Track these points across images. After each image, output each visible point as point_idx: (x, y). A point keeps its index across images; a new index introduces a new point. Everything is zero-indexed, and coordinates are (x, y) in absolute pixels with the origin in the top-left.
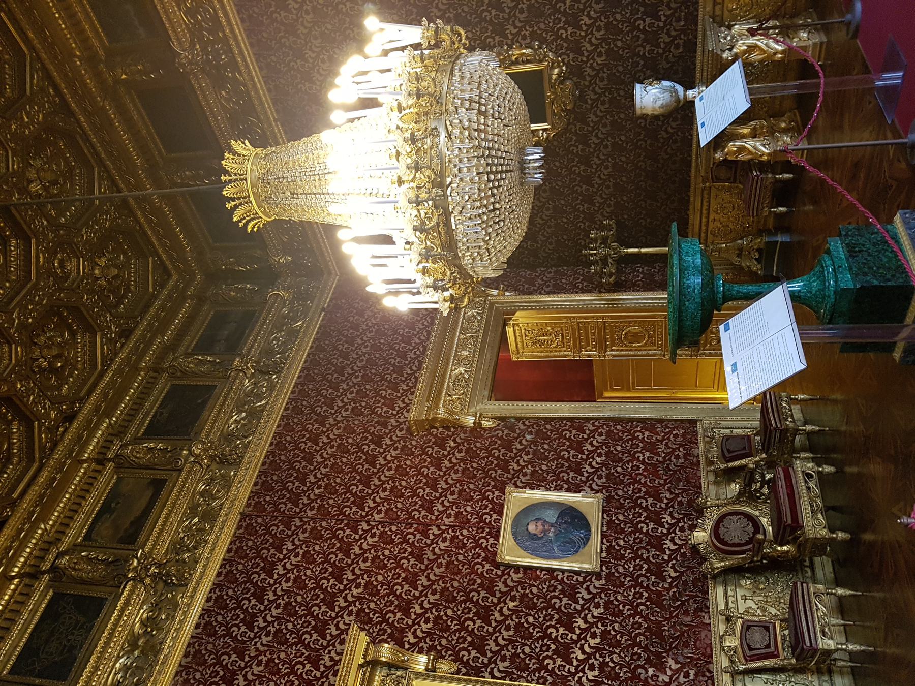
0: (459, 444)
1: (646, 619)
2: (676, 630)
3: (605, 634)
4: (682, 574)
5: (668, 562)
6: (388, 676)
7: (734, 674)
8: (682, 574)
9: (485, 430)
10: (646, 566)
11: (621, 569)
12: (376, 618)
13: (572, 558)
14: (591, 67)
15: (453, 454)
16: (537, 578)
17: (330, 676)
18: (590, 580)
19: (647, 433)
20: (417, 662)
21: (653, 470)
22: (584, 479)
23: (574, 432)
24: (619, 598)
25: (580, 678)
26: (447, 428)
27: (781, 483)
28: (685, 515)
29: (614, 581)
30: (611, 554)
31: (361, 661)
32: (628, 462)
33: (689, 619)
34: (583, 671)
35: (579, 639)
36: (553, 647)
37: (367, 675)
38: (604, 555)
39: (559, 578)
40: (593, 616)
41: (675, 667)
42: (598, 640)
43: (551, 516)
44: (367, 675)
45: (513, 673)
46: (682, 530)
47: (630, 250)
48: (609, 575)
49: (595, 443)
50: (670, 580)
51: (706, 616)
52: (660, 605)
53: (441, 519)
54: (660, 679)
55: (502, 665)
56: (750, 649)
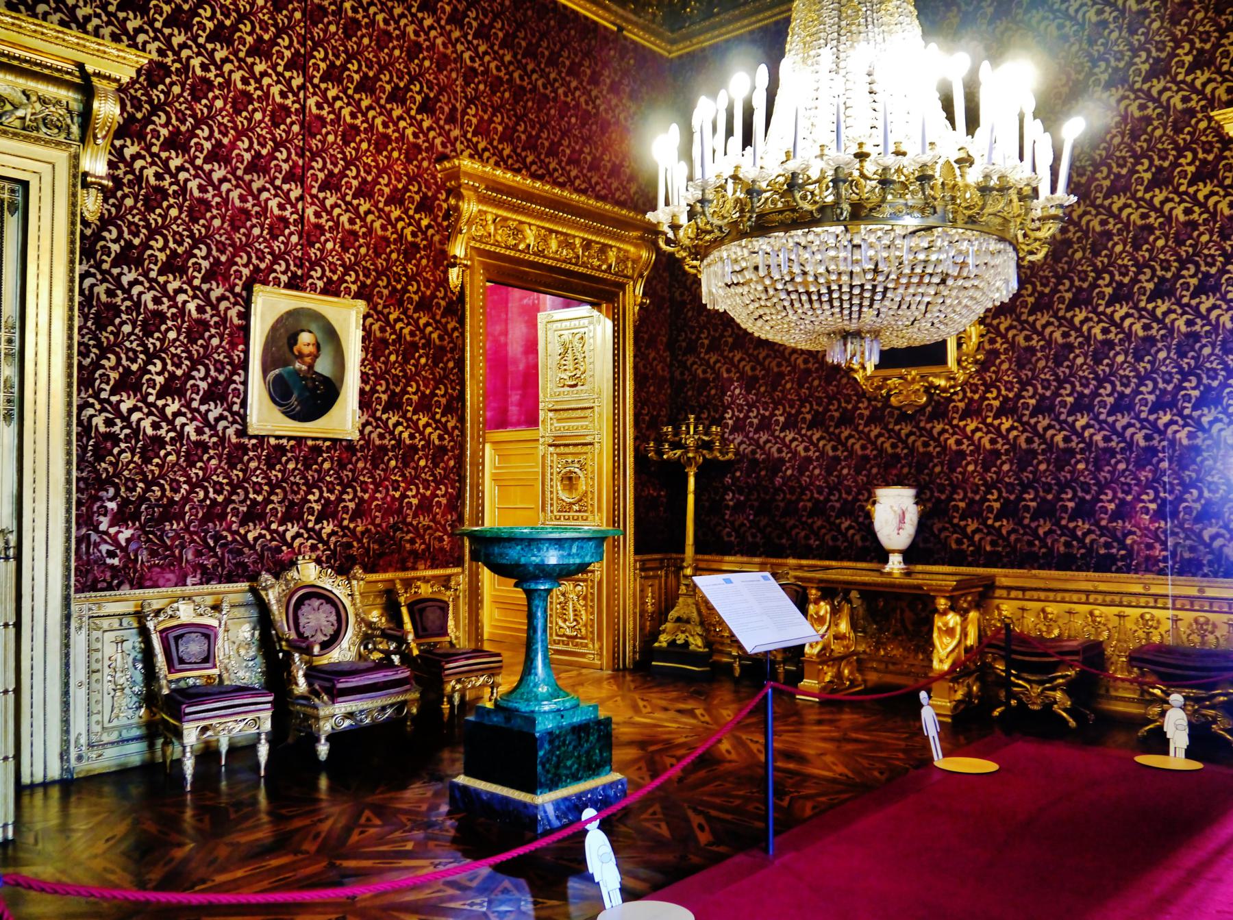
0: (424, 233)
1: (186, 499)
2: (173, 539)
3: (159, 442)
4: (252, 547)
5: (268, 528)
6: (70, 112)
7: (140, 616)
8: (252, 547)
9: (446, 272)
10: (260, 498)
11: (253, 465)
12: (157, 94)
14: (944, 431)
15: (410, 224)
16: (233, 346)
17: (59, 15)
18: (234, 422)
19: (444, 501)
20: (95, 157)
21: (395, 509)
22: (378, 414)
23: (443, 401)
24: (214, 462)
25: (92, 406)
26: (447, 216)
27: (391, 676)
29: (236, 455)
30: (275, 452)
31: (90, 68)
32: (403, 475)
33: (190, 557)
34: (103, 410)
35: (149, 405)
36: (134, 367)
37: (67, 77)
39: (236, 378)
40: (183, 425)
41: (122, 538)
42: (150, 431)
43: (323, 366)
44: (67, 77)
45: (91, 307)
46: (314, 548)
47: (692, 481)
48: (244, 449)
49: (429, 430)
50: (242, 531)
51: (196, 580)
52: (208, 517)
54: (102, 518)
55: (101, 289)
56: (177, 638)
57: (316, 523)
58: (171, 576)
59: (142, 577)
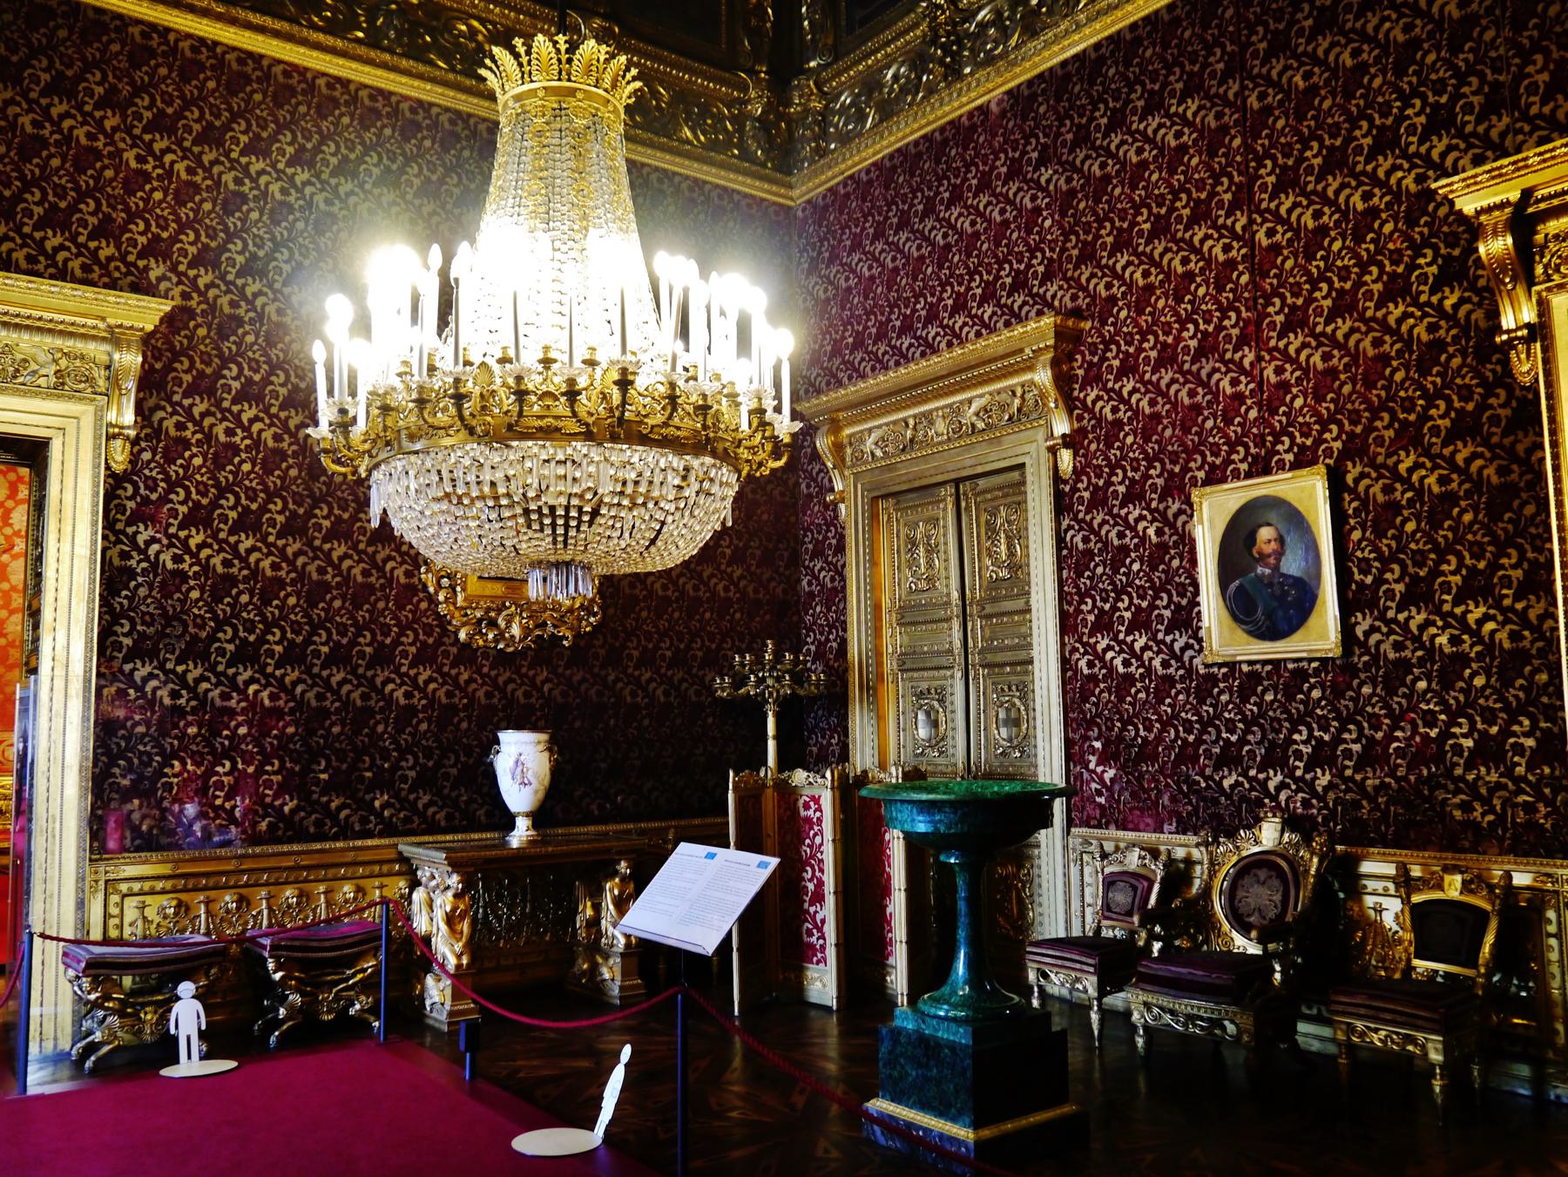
1: (1159, 739)
2: (1149, 782)
5: (1245, 774)
13: (1225, 614)
21: (1430, 753)
24: (1181, 697)
28: (1333, 812)
29: (1205, 685)
30: (1248, 680)
33: (1167, 802)
38: (1245, 668)
40: (1151, 659)
43: (1292, 565)
51: (1173, 828)
53: (1273, 358)
57: (1306, 771)
58: (1149, 820)
59: (1125, 819)
